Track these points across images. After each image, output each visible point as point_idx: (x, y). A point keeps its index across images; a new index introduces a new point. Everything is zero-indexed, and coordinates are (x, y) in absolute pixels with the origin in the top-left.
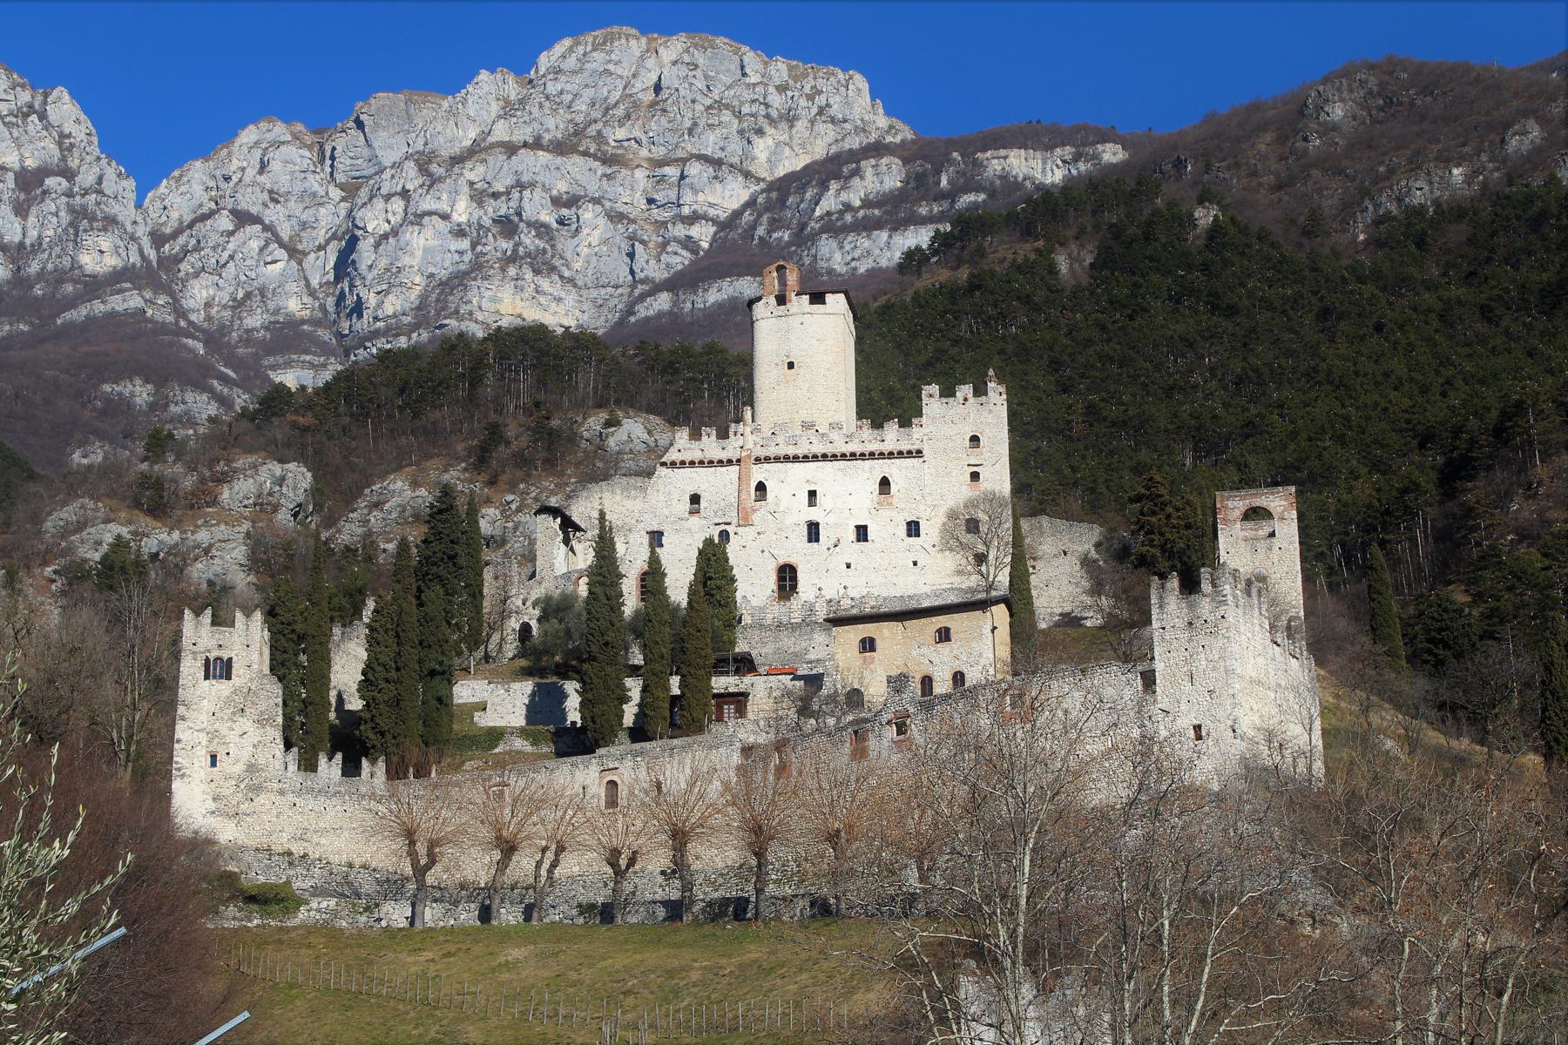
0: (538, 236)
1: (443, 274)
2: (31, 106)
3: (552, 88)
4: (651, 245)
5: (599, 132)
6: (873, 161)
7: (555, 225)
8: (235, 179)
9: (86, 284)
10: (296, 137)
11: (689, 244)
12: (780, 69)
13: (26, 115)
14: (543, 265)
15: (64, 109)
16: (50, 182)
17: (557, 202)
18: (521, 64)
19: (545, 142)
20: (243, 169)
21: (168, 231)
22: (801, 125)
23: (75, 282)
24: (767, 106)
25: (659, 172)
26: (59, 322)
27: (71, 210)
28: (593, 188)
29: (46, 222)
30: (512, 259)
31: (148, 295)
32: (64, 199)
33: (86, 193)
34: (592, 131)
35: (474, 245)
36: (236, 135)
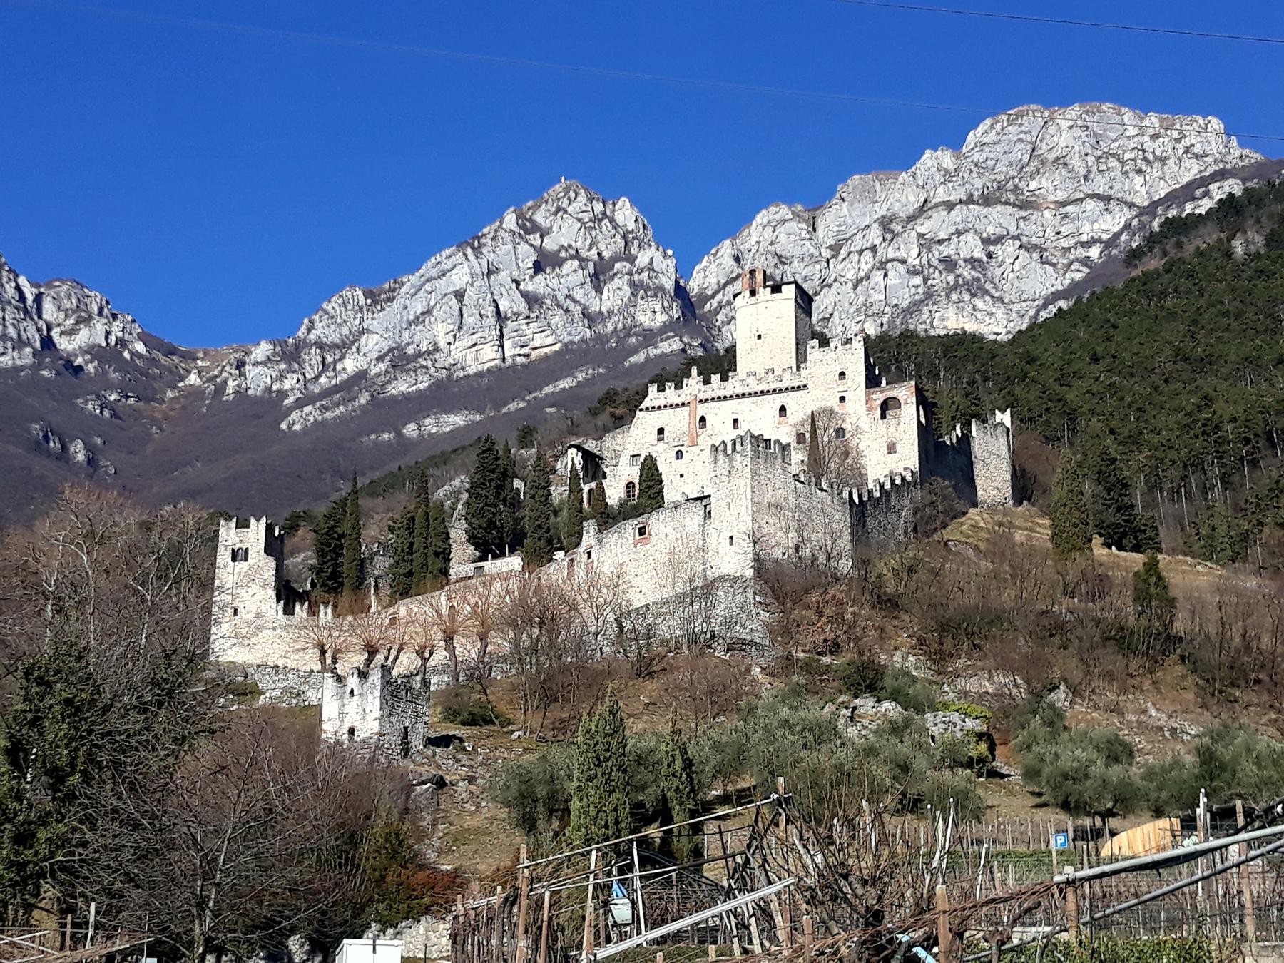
0: (973, 268)
1: (905, 304)
2: (604, 214)
3: (977, 157)
5: (1016, 186)
6: (1217, 184)
7: (985, 259)
9: (645, 337)
10: (796, 215)
11: (1085, 261)
12: (1153, 120)
14: (976, 289)
15: (626, 213)
17: (986, 242)
18: (955, 144)
19: (976, 198)
20: (759, 242)
21: (710, 293)
22: (1171, 163)
23: (636, 335)
24: (1144, 151)
25: (1062, 210)
26: (627, 364)
27: (632, 284)
28: (1013, 229)
29: (614, 295)
30: (955, 287)
31: (685, 340)
32: (627, 277)
33: (641, 271)
34: (1010, 186)
35: (925, 280)
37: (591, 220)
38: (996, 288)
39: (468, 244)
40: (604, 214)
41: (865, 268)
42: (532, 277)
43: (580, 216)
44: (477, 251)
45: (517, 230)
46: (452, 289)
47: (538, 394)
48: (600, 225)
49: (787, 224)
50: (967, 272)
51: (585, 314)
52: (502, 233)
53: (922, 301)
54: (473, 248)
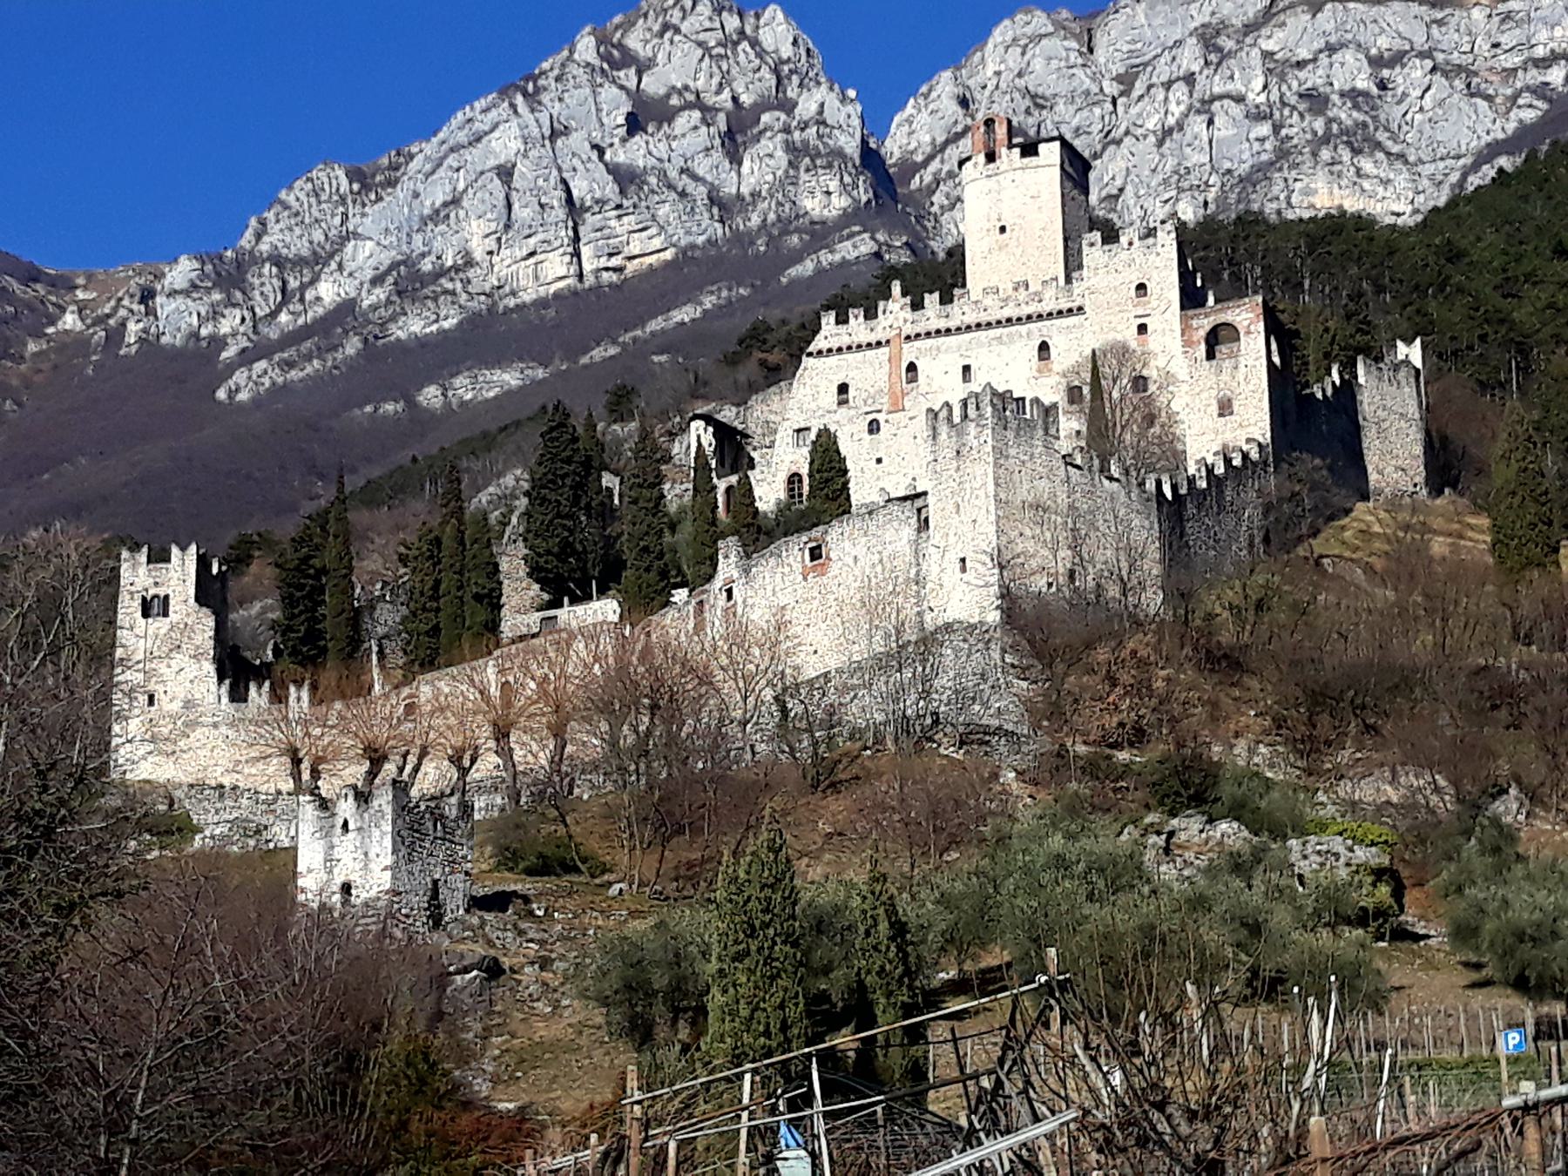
0: (1356, 107)
1: (1243, 169)
2: (742, 32)
4: (1499, 100)
7: (1375, 91)
8: (990, 87)
9: (813, 234)
10: (1060, 26)
11: (1542, 91)
13: (736, 44)
14: (1361, 141)
15: (777, 31)
16: (766, 118)
17: (1377, 62)
20: (998, 73)
21: (919, 158)
23: (798, 230)
27: (790, 147)
28: (1420, 40)
29: (761, 167)
30: (1326, 139)
31: (880, 237)
32: (780, 137)
33: (804, 126)
35: (1276, 129)
36: (988, 33)
37: (719, 44)
38: (1394, 138)
39: (517, 88)
40: (742, 32)
41: (1176, 110)
42: (624, 141)
43: (702, 37)
44: (533, 99)
45: (597, 62)
46: (492, 163)
47: (639, 333)
48: (735, 54)
49: (1044, 42)
50: (1345, 114)
51: (714, 199)
52: (573, 69)
53: (1272, 164)
54: (525, 94)
